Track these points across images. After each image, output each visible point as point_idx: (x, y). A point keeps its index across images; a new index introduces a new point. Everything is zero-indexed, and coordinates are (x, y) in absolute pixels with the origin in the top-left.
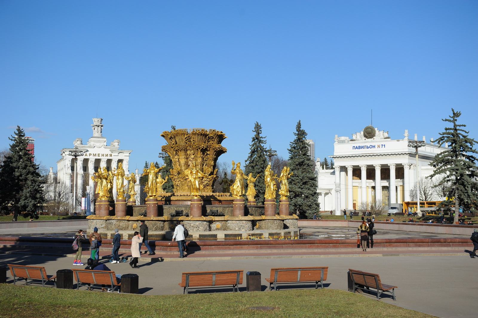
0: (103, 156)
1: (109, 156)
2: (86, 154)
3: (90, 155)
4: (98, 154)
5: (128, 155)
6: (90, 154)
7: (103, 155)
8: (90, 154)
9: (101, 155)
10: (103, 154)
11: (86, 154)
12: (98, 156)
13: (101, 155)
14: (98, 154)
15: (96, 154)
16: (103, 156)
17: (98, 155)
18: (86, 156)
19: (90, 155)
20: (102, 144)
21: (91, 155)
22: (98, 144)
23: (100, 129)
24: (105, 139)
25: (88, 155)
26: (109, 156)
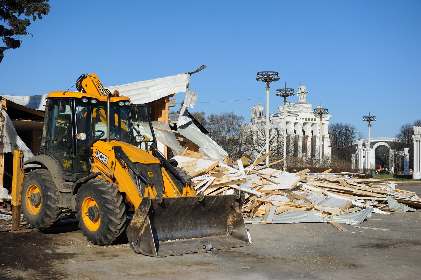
0: (309, 120)
1: (314, 120)
2: (297, 118)
3: (300, 119)
4: (306, 118)
5: (329, 119)
6: (299, 118)
7: (309, 119)
8: (299, 118)
9: (307, 120)
10: (309, 119)
11: (297, 118)
12: (306, 120)
13: (307, 120)
14: (306, 118)
15: (304, 118)
16: (309, 120)
17: (306, 119)
18: (297, 120)
19: (300, 119)
20: (309, 109)
21: (300, 119)
22: (305, 110)
23: (305, 96)
24: (311, 105)
25: (298, 119)
26: (314, 120)
